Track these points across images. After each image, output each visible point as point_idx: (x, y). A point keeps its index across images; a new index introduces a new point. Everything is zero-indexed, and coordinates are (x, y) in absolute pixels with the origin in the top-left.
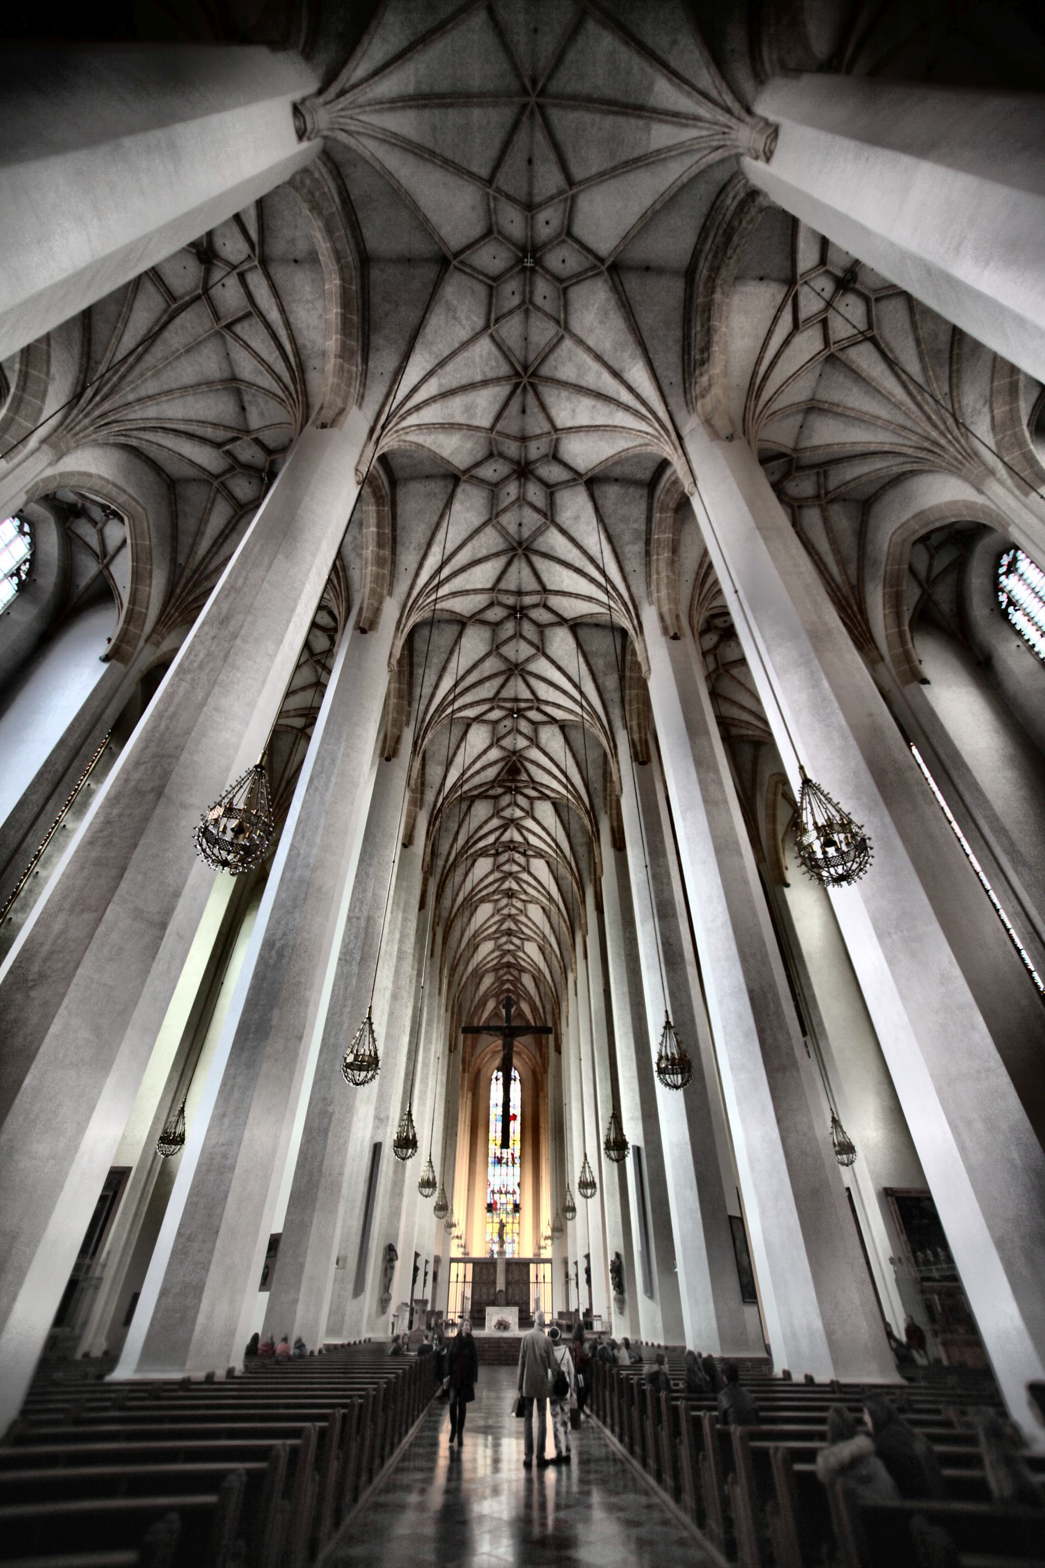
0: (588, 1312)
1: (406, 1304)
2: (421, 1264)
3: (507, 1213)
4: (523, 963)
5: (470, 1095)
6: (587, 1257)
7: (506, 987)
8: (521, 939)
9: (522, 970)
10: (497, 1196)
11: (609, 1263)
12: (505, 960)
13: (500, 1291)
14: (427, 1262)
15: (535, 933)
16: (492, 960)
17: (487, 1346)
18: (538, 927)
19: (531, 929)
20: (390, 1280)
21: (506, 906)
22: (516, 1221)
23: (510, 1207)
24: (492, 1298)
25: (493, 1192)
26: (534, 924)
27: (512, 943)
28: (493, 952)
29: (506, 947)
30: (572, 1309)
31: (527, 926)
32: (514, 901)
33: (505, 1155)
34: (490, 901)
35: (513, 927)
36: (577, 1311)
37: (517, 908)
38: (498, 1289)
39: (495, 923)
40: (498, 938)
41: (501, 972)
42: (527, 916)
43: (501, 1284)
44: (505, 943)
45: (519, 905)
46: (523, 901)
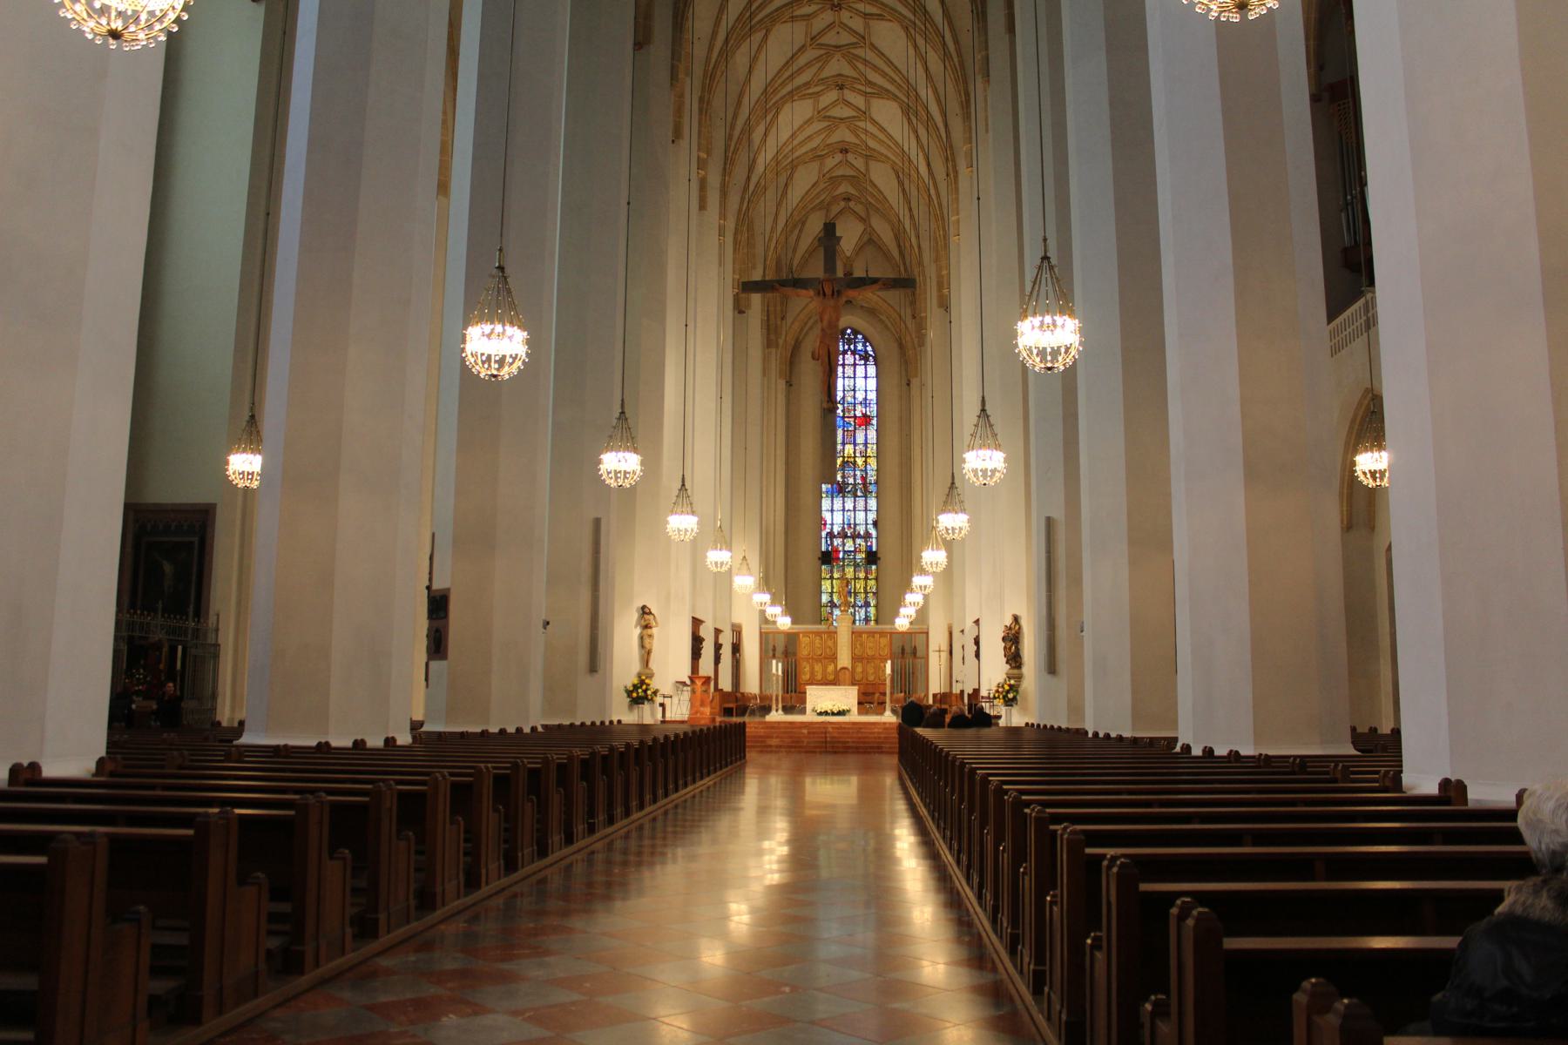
0: (976, 691)
1: (684, 684)
2: (706, 633)
3: (856, 566)
4: (872, 144)
5: (782, 384)
6: (977, 622)
8: (865, 94)
9: (870, 156)
10: (837, 542)
11: (1003, 629)
12: (835, 138)
14: (718, 632)
15: (892, 81)
16: (809, 138)
17: (805, 731)
18: (896, 69)
19: (884, 74)
20: (649, 653)
21: (831, 26)
22: (874, 576)
23: (861, 556)
24: (832, 677)
25: (831, 535)
26: (889, 62)
27: (848, 104)
28: (809, 122)
29: (839, 112)
30: (956, 690)
31: (875, 68)
32: (845, 15)
33: (851, 481)
34: (793, 19)
35: (847, 70)
36: (962, 692)
37: (852, 31)
38: (838, 668)
39: (809, 64)
40: (818, 94)
41: (830, 162)
42: (873, 47)
43: (844, 660)
44: (834, 104)
45: (857, 24)
46: (866, 16)
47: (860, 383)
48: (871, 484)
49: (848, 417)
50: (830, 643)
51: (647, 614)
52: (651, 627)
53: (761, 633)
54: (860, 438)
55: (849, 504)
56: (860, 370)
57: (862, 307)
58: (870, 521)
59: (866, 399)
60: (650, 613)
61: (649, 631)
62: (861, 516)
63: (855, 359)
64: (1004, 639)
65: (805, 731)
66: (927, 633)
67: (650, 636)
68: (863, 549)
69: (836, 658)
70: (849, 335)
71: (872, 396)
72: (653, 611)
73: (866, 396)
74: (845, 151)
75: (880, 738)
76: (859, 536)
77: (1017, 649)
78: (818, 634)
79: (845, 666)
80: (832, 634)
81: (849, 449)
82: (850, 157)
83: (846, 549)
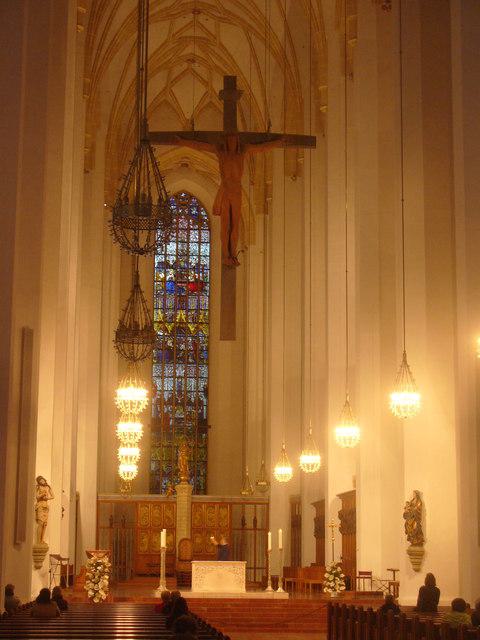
7: (189, 50)
13: (184, 539)
17: (205, 609)
41: (181, 22)
47: (194, 247)
48: (202, 350)
49: (181, 282)
50: (169, 513)
51: (43, 485)
52: (46, 500)
53: (98, 503)
54: (192, 303)
55: (180, 372)
56: (194, 236)
57: (197, 171)
58: (201, 388)
59: (198, 264)
60: (46, 485)
61: (44, 503)
62: (193, 382)
63: (189, 223)
64: (405, 516)
65: (205, 609)
66: (268, 504)
67: (46, 509)
68: (194, 416)
69: (175, 529)
70: (183, 198)
71: (206, 261)
72: (49, 483)
73: (199, 261)
74: (196, 12)
75: (282, 615)
76: (189, 403)
77: (419, 526)
78: (157, 504)
79: (185, 537)
80: (172, 505)
81: (181, 315)
82: (201, 18)
83: (177, 416)
